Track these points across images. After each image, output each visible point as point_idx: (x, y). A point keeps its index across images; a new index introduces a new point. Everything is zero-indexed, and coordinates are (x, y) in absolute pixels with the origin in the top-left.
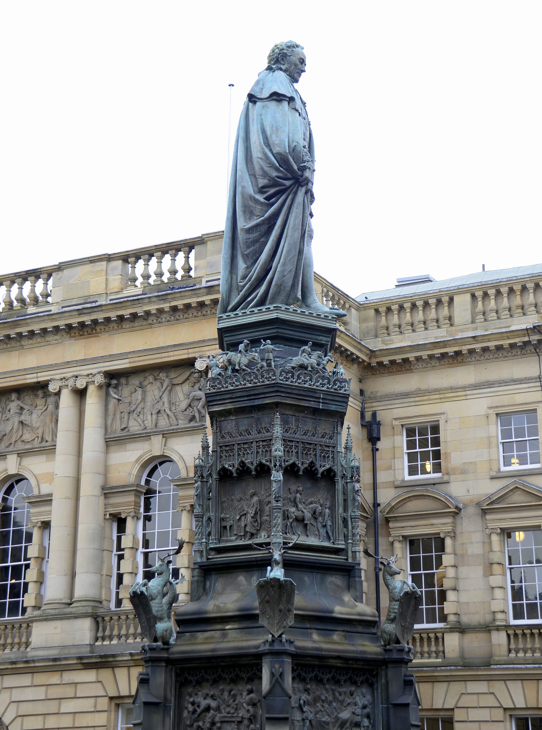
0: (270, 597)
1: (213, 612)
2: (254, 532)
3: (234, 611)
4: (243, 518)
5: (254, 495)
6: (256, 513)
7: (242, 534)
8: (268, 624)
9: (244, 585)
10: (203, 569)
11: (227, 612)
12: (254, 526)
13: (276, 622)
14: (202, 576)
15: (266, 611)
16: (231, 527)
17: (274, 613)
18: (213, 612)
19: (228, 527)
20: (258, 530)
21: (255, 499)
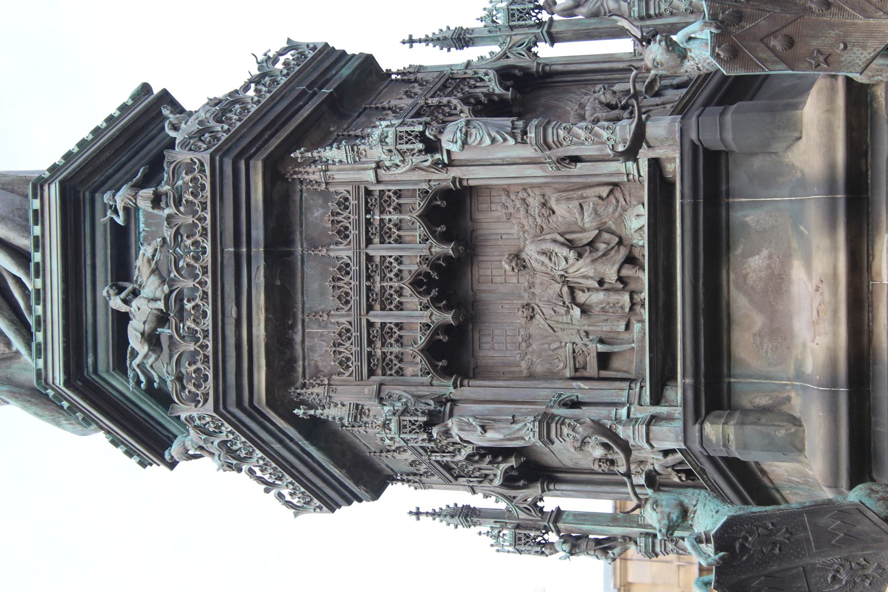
0: (773, 34)
1: (835, 334)
2: (623, 252)
3: (834, 248)
4: (581, 297)
5: (518, 260)
6: (570, 244)
7: (627, 297)
8: (864, 47)
9: (770, 257)
10: (708, 413)
11: (835, 275)
12: (604, 255)
13: (861, 20)
14: (730, 416)
15: (819, 51)
16: (601, 341)
17: (832, 26)
18: (835, 334)
19: (601, 348)
20: (621, 242)
21: (531, 252)
